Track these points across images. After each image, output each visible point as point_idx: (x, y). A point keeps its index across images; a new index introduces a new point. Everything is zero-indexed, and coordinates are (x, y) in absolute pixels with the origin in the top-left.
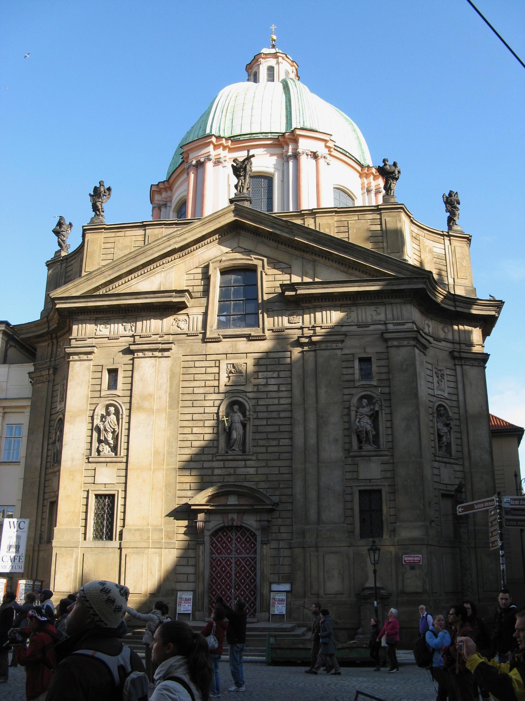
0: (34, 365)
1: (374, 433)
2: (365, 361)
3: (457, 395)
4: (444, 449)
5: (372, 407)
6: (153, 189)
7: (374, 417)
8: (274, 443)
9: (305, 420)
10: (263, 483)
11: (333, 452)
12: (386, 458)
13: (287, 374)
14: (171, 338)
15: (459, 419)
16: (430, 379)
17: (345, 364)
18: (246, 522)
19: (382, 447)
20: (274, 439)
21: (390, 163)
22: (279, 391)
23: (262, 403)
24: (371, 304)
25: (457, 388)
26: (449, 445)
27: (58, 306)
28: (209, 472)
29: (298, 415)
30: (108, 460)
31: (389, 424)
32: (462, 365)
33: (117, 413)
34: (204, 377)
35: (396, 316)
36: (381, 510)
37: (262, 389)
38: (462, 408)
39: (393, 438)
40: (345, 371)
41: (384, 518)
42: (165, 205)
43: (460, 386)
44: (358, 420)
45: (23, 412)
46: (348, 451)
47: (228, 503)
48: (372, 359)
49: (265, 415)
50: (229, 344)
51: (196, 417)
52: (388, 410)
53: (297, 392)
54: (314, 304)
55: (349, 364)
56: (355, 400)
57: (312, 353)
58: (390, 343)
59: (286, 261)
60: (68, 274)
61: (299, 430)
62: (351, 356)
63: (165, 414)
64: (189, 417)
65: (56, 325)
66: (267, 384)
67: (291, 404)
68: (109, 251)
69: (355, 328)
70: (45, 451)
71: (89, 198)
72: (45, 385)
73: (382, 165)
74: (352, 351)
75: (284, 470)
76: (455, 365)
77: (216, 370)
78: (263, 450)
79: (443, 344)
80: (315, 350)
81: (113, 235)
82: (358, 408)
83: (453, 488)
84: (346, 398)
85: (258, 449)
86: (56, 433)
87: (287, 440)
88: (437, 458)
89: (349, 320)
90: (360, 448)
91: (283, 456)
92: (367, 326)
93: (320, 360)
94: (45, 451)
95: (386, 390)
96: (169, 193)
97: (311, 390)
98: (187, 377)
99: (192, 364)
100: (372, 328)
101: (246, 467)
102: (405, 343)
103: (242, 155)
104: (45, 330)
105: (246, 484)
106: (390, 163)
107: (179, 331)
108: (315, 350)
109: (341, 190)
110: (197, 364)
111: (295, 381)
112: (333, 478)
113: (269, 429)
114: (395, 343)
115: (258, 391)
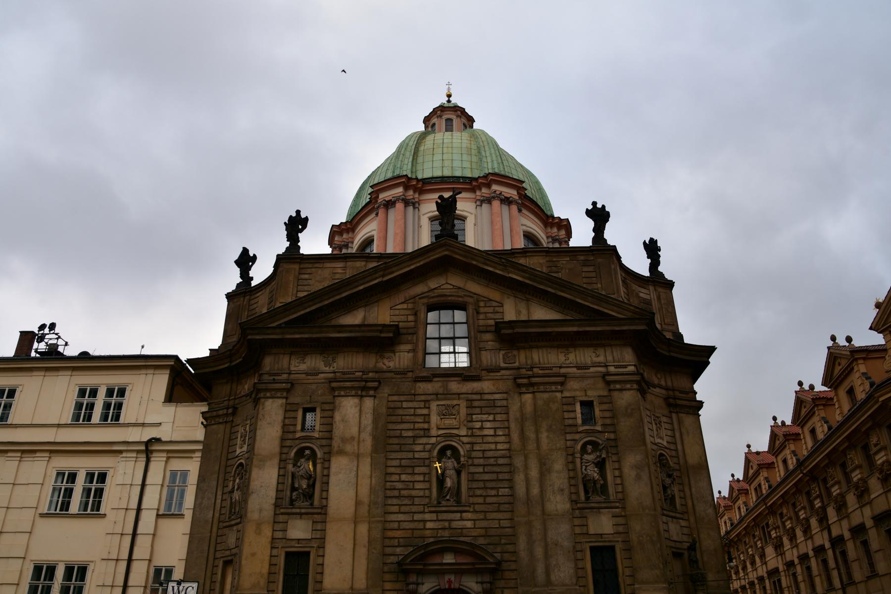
1: (602, 482)
2: (587, 405)
3: (675, 443)
4: (668, 501)
5: (598, 454)
7: (601, 465)
8: (493, 492)
9: (526, 467)
10: (482, 538)
11: (559, 503)
12: (617, 510)
13: (504, 417)
14: (377, 376)
15: (679, 470)
16: (650, 426)
17: (565, 407)
18: (465, 584)
19: (611, 498)
20: (492, 488)
21: (599, 206)
22: (495, 435)
23: (478, 448)
24: (588, 346)
25: (674, 437)
26: (673, 496)
27: (249, 337)
28: (421, 525)
29: (518, 462)
30: (303, 511)
31: (617, 473)
32: (677, 413)
33: (313, 457)
34: (412, 418)
35: (616, 358)
36: (615, 570)
37: (478, 433)
38: (681, 458)
39: (623, 488)
40: (566, 415)
41: (620, 579)
43: (678, 435)
44: (584, 467)
45: (192, 458)
46: (574, 502)
47: (444, 561)
49: (481, 461)
50: (440, 384)
52: (615, 458)
53: (515, 437)
55: (570, 408)
56: (579, 447)
57: (529, 396)
58: (612, 387)
59: (498, 299)
60: (252, 307)
61: (519, 479)
62: (571, 399)
63: (369, 460)
64: (396, 463)
66: (482, 428)
67: (509, 450)
68: (306, 282)
69: (575, 370)
70: (219, 501)
71: (284, 227)
72: (222, 427)
73: (590, 207)
75: (505, 523)
77: (425, 411)
78: (481, 500)
79: (657, 390)
80: (533, 392)
81: (310, 266)
82: (582, 455)
83: (686, 545)
84: (569, 443)
85: (475, 500)
86: (234, 481)
87: (507, 490)
89: (567, 362)
90: (587, 498)
91: (502, 508)
92: (587, 367)
93: (540, 402)
94: (219, 501)
95: (612, 436)
96: (350, 235)
98: (393, 418)
99: (399, 405)
100: (592, 370)
101: (462, 519)
102: (628, 386)
104: (226, 365)
105: (462, 539)
106: (599, 206)
108: (533, 392)
109: (528, 236)
110: (405, 405)
111: (513, 425)
112: (561, 532)
114: (618, 386)
115: (472, 435)
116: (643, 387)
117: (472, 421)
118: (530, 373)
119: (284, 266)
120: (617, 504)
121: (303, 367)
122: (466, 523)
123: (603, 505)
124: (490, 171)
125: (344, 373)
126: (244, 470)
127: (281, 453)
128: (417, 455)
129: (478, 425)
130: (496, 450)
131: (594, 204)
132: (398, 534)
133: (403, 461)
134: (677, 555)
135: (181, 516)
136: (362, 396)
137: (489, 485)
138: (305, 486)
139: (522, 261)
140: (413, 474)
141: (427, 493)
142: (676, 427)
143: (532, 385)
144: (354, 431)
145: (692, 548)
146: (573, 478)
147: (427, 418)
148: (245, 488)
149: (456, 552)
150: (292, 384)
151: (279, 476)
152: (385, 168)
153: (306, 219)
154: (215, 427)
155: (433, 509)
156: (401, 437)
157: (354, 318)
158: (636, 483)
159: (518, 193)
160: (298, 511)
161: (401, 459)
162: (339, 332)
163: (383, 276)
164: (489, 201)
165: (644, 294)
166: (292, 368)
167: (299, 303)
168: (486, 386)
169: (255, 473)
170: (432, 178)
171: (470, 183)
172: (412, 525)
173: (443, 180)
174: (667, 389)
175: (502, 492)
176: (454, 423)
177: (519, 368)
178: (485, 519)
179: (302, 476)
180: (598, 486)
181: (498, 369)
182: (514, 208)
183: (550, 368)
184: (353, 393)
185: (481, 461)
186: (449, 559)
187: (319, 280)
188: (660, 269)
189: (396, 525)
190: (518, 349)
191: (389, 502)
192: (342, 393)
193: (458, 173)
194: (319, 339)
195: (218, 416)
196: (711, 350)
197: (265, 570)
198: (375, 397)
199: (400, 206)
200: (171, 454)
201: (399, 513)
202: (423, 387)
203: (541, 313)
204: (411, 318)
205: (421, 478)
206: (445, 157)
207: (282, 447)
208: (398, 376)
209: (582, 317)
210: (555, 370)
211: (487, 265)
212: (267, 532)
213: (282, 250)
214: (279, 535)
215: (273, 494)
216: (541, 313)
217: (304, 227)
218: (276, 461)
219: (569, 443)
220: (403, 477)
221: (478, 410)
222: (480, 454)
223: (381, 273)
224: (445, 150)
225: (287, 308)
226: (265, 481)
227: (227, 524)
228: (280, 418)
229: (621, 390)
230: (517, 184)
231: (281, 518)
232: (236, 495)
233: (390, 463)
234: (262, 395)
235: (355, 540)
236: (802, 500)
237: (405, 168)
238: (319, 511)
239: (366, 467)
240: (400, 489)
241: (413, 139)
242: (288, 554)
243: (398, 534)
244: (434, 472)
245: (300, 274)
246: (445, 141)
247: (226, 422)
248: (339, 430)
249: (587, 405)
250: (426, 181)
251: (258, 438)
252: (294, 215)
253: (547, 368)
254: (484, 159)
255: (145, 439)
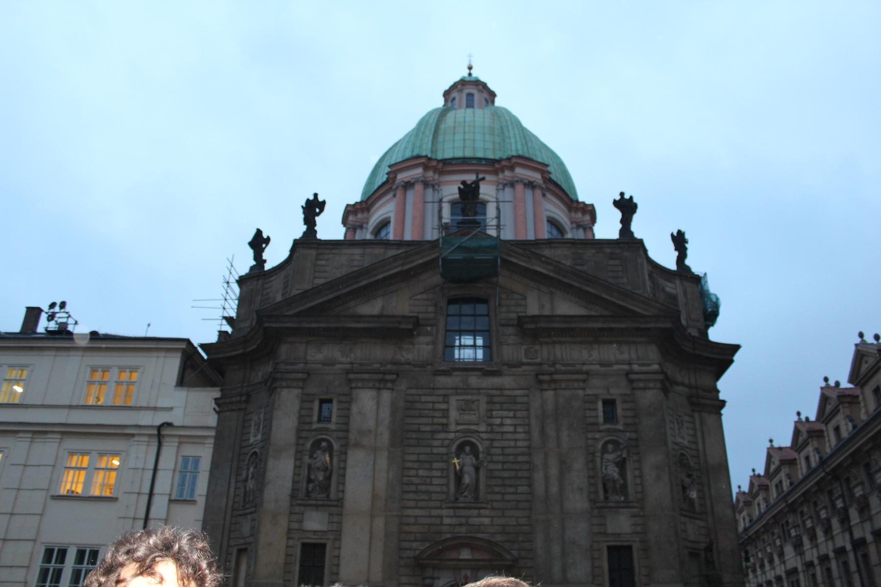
0: (222, 390)
1: (622, 482)
3: (696, 443)
5: (619, 453)
6: (349, 209)
8: (512, 490)
11: (577, 502)
12: (635, 510)
13: (525, 413)
20: (511, 486)
21: (627, 197)
22: (515, 432)
25: (695, 436)
28: (438, 521)
29: (538, 459)
30: (320, 503)
31: (637, 473)
36: (631, 570)
37: (497, 429)
40: (588, 413)
41: (636, 579)
42: (361, 227)
43: (699, 434)
46: (593, 501)
47: (461, 557)
48: (617, 402)
49: (501, 458)
51: (422, 457)
53: (536, 434)
54: (554, 339)
56: (600, 446)
58: (635, 385)
61: (539, 476)
63: (386, 454)
64: (413, 457)
65: (255, 346)
66: (502, 425)
67: (529, 447)
69: (597, 367)
70: (232, 489)
71: (301, 210)
73: (618, 198)
74: (594, 392)
75: (523, 521)
76: (693, 411)
77: (444, 406)
78: (499, 497)
79: (680, 389)
80: (555, 389)
81: (328, 251)
82: (603, 454)
83: (703, 546)
84: (590, 442)
85: (494, 497)
86: (248, 470)
88: (684, 513)
90: (606, 498)
94: (232, 489)
95: (634, 436)
96: (365, 215)
97: (551, 432)
100: (616, 367)
101: (479, 516)
102: (652, 385)
103: (470, 178)
104: (241, 351)
105: (480, 535)
106: (627, 197)
107: (403, 360)
109: (553, 222)
110: (423, 399)
112: (579, 531)
113: (506, 474)
115: (492, 432)
116: (667, 385)
117: (491, 417)
118: (552, 369)
119: (301, 251)
120: (636, 504)
121: (319, 357)
122: (483, 519)
123: (622, 505)
124: (514, 154)
125: (361, 365)
126: (258, 460)
127: (297, 444)
128: (435, 451)
129: (498, 421)
130: (516, 447)
131: (622, 194)
132: (415, 529)
133: (421, 456)
134: (694, 555)
135: (193, 502)
136: (379, 389)
137: (507, 482)
138: (321, 478)
139: (547, 252)
140: (431, 469)
141: (445, 488)
142: (698, 426)
143: (555, 381)
144: (371, 423)
145: (709, 549)
146: (593, 477)
147: (445, 413)
148: (261, 478)
149: (473, 548)
150: (309, 374)
151: (295, 467)
152: (403, 146)
153: (324, 203)
154: (228, 414)
155: (450, 505)
156: (419, 431)
157: (372, 308)
158: (655, 484)
159: (543, 177)
160: (313, 502)
161: (419, 454)
162: (358, 322)
163: (403, 265)
164: (512, 184)
165: (670, 287)
166: (309, 358)
167: (317, 291)
168: (506, 381)
169: (271, 463)
170: (453, 159)
171: (493, 165)
172: (428, 521)
173: (464, 161)
174: (690, 387)
175: (521, 489)
176: (474, 418)
177: (540, 364)
178: (503, 516)
179: (318, 469)
180: (618, 486)
181: (520, 364)
182: (538, 192)
183: (573, 365)
184: (371, 385)
185: (501, 458)
186: (465, 554)
187: (337, 267)
188: (688, 262)
189: (412, 520)
190: (541, 344)
191: (407, 496)
192: (360, 385)
193: (480, 155)
194: (337, 329)
195: (232, 403)
196: (736, 348)
197: (281, 560)
198: (393, 389)
199: (419, 187)
200: (183, 440)
201: (416, 507)
202: (442, 380)
203: (566, 307)
204: (431, 309)
205: (439, 474)
206: (467, 136)
207: (299, 438)
208: (417, 369)
209: (606, 313)
210: (578, 367)
211: (511, 256)
212: (283, 522)
213: (299, 235)
214: (295, 526)
215: (289, 485)
216: (566, 307)
217: (322, 210)
218: (292, 452)
219: (590, 442)
220: (421, 472)
221: (498, 406)
222: (499, 451)
223: (400, 262)
224: (467, 129)
225: (305, 295)
226: (282, 472)
227: (240, 512)
228: (296, 408)
229: (644, 389)
230: (542, 168)
231: (297, 509)
232: (251, 484)
233: (407, 457)
234: (277, 384)
235: (371, 533)
236: (824, 499)
237: (424, 147)
238: (335, 503)
239: (383, 462)
240: (417, 484)
241: (433, 117)
242: (304, 545)
243: (415, 529)
244: (452, 468)
245: (317, 259)
246: (467, 119)
247: (240, 409)
248: (356, 422)
249: (609, 404)
250: (446, 162)
251: (274, 428)
252: (311, 198)
253: (569, 365)
254: (508, 141)
255: (158, 423)
